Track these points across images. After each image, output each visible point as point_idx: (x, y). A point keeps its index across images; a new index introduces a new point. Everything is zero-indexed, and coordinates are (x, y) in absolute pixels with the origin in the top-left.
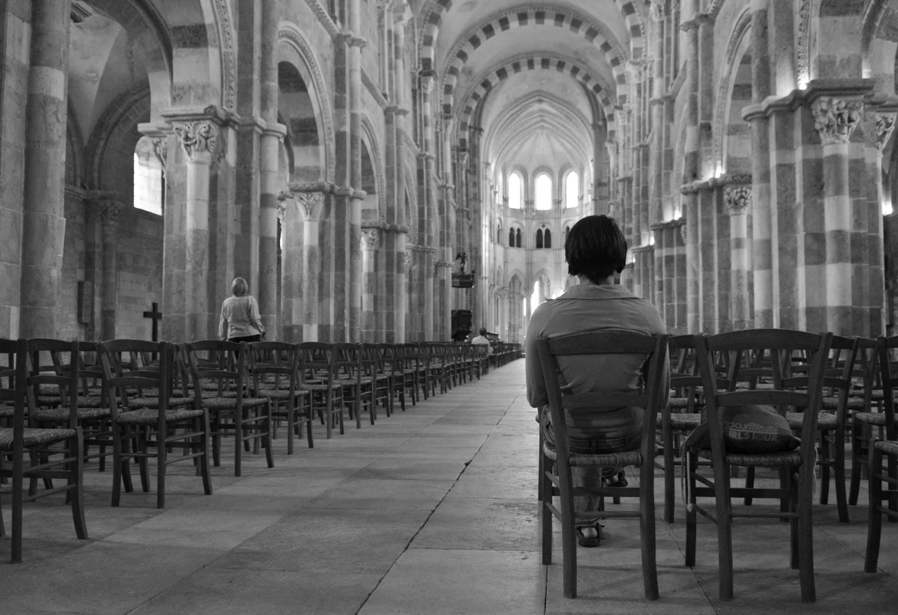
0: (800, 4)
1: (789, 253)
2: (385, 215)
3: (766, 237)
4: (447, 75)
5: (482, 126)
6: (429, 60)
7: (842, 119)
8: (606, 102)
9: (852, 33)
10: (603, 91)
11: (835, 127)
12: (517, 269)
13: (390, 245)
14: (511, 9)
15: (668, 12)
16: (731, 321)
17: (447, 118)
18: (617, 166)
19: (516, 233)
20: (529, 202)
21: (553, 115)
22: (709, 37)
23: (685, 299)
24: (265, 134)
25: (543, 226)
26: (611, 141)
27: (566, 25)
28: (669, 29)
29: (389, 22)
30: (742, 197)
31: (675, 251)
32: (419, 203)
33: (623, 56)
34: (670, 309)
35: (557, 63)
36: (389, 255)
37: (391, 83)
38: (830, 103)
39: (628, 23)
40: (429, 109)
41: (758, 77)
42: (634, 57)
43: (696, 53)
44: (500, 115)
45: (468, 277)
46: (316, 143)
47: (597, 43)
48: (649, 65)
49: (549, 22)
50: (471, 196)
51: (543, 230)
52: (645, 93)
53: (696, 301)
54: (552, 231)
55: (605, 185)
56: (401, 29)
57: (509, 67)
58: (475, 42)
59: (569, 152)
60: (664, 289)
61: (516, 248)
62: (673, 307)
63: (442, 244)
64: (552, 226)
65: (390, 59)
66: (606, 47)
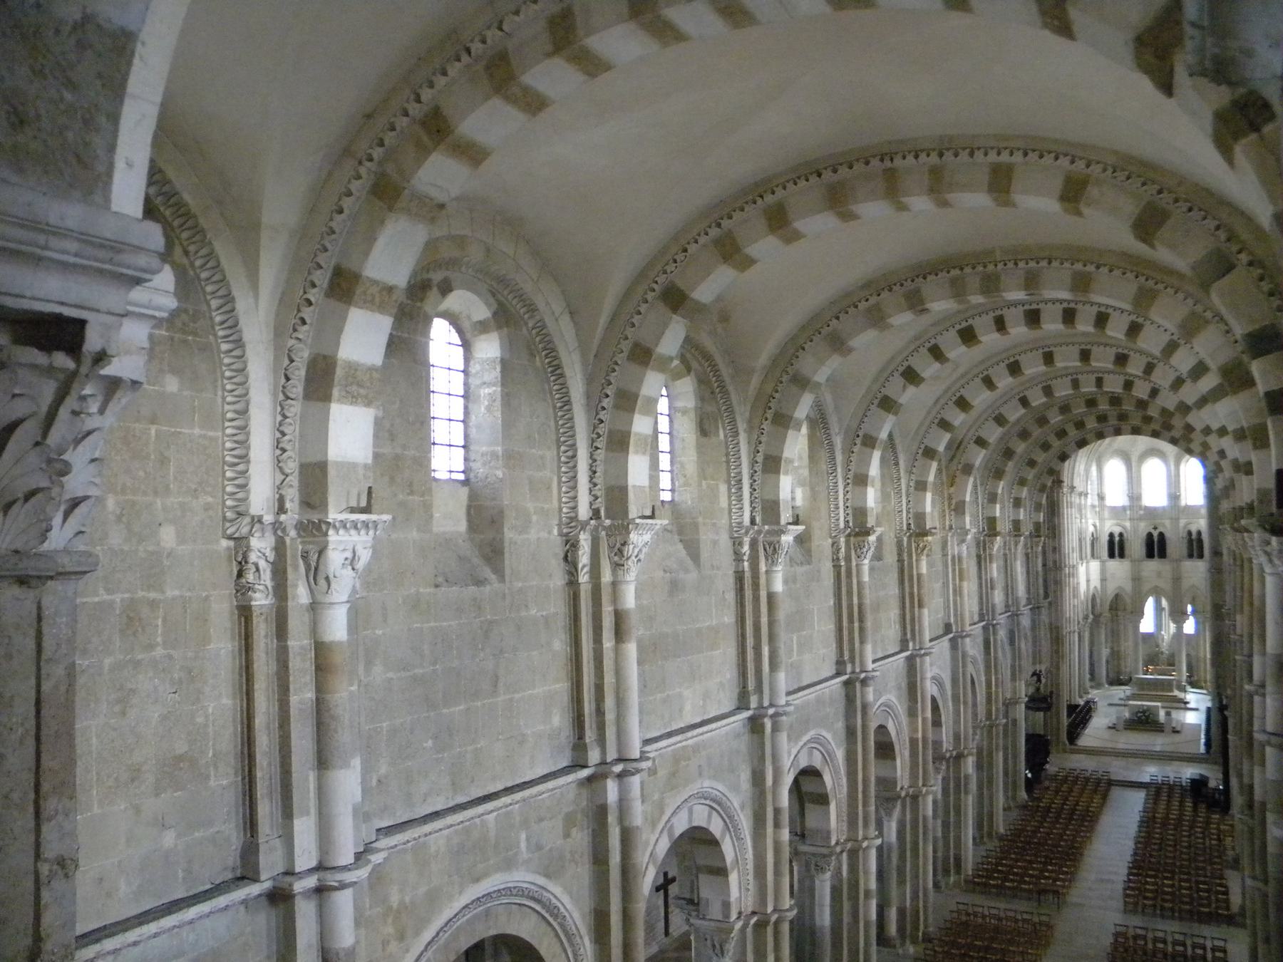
2: (951, 741)
4: (1015, 487)
6: (994, 518)
12: (1120, 588)
19: (1117, 539)
20: (1135, 497)
25: (1155, 528)
29: (953, 548)
32: (986, 675)
37: (956, 610)
46: (894, 759)
50: (1050, 564)
51: (1155, 534)
54: (1167, 535)
56: (965, 548)
61: (1117, 558)
63: (1013, 678)
64: (1167, 528)
65: (954, 585)
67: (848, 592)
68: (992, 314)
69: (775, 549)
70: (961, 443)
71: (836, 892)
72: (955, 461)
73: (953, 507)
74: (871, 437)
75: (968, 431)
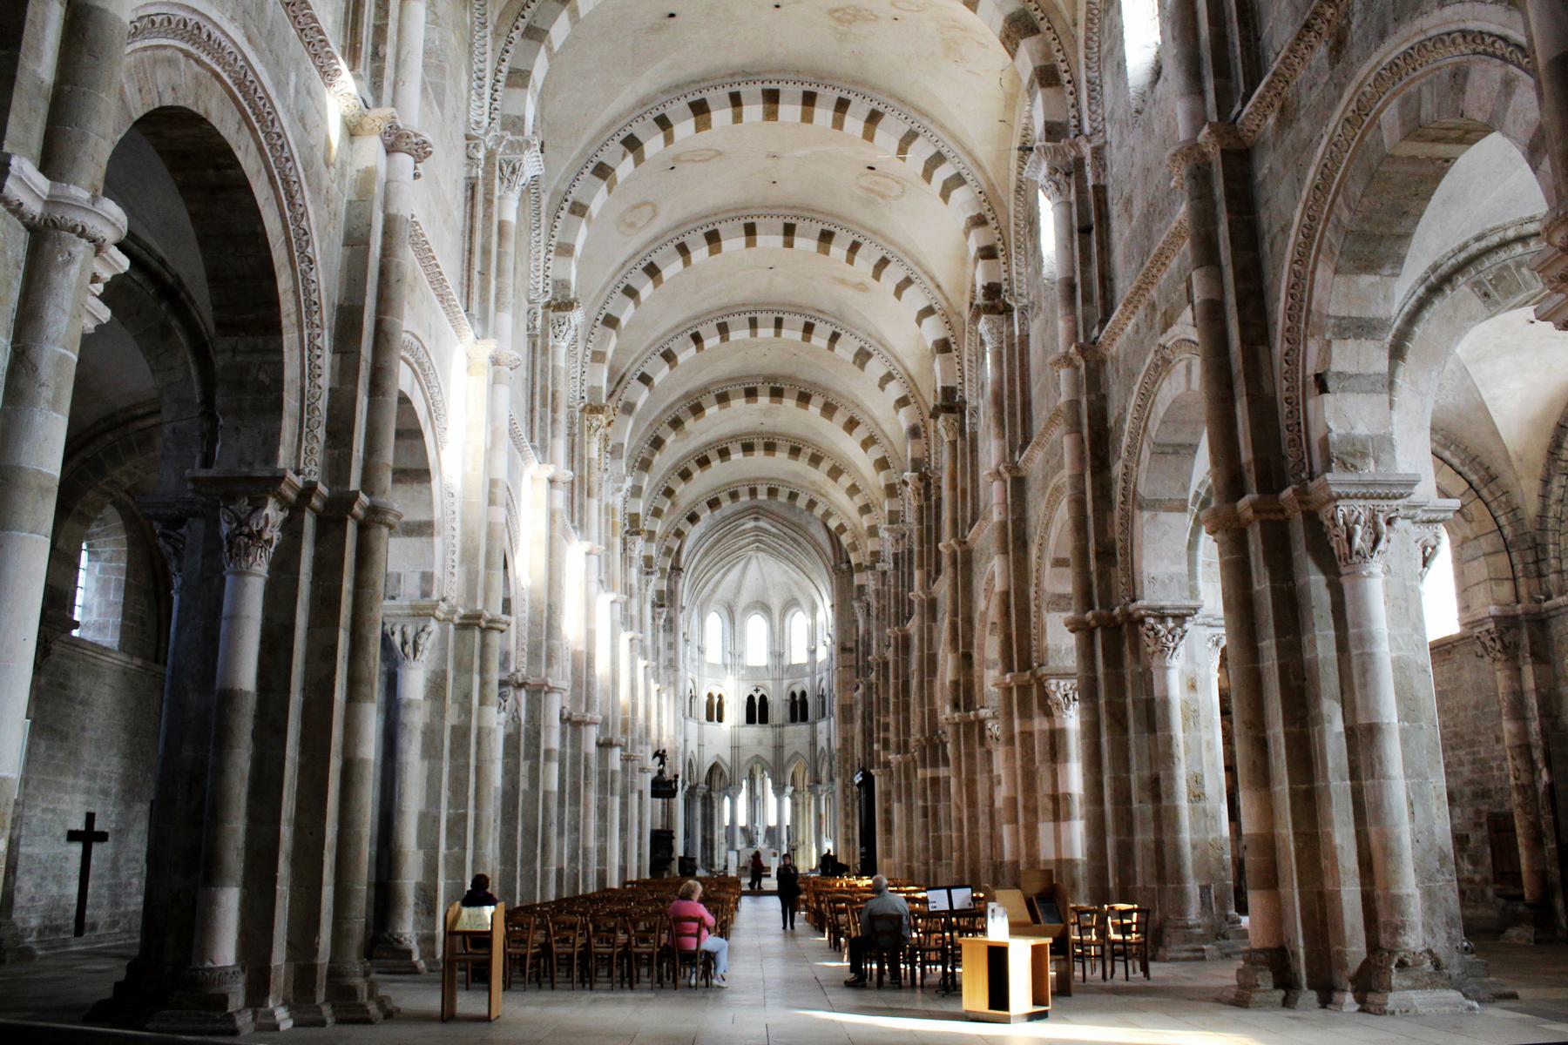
1: (1032, 811)
3: (1012, 794)
4: (649, 518)
12: (718, 756)
13: (603, 760)
14: (734, 438)
15: (927, 497)
17: (647, 573)
18: (868, 632)
21: (774, 535)
24: (551, 690)
25: (757, 690)
26: (859, 598)
28: (929, 515)
31: (942, 772)
36: (603, 773)
37: (607, 566)
38: (1058, 685)
39: (881, 479)
40: (634, 572)
42: (891, 522)
43: (955, 578)
44: (700, 539)
45: (670, 782)
47: (845, 481)
52: (903, 566)
53: (961, 839)
54: (769, 698)
55: (850, 650)
58: (685, 475)
59: (796, 583)
60: (930, 815)
62: (939, 837)
65: (607, 538)
66: (853, 490)
67: (542, 371)
68: (728, 89)
69: (514, 169)
70: (622, 377)
71: (511, 743)
72: (615, 398)
73: (609, 449)
74: (581, 205)
75: (632, 364)
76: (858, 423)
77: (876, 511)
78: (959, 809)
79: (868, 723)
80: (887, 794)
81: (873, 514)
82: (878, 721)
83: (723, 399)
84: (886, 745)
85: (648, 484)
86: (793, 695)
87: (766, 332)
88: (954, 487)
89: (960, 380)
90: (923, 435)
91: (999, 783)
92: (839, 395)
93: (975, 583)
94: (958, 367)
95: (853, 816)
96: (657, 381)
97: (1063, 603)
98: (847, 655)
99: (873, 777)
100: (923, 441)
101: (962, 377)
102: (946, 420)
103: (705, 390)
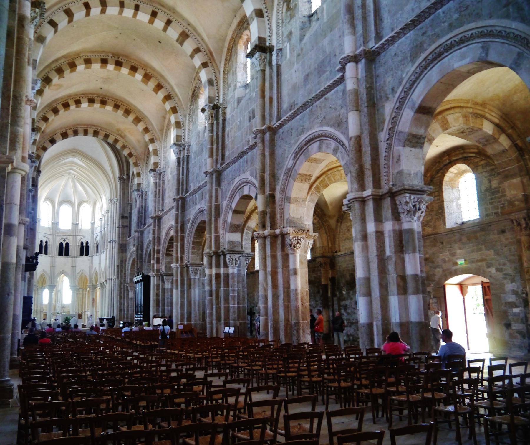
0: (385, 136)
5: (41, 169)
7: (416, 207)
8: (136, 165)
9: (418, 159)
10: (134, 157)
11: (412, 212)
12: (44, 271)
14: (84, 95)
15: (217, 118)
16: (291, 322)
19: (44, 244)
20: (55, 224)
22: (272, 141)
23: (228, 303)
25: (64, 240)
26: (138, 190)
27: (120, 112)
28: (218, 129)
30: (298, 243)
31: (222, 271)
33: (157, 137)
34: (218, 309)
35: (104, 135)
38: (410, 197)
41: (358, 176)
42: (177, 140)
48: (187, 147)
49: (109, 108)
55: (126, 218)
57: (70, 132)
58: (56, 111)
61: (43, 255)
62: (220, 308)
66: (146, 130)
76: (162, 87)
77: (157, 142)
78: (266, 290)
79: (139, 252)
80: (158, 286)
81: (156, 143)
82: (154, 249)
83: (88, 62)
84: (158, 261)
85: (41, 103)
86: (82, 243)
87: (128, 12)
88: (263, 97)
89: (269, 34)
90: (215, 84)
91: (295, 273)
92: (154, 70)
93: (279, 152)
94: (268, 26)
95: (124, 298)
96: (60, 27)
97: (414, 141)
98: (125, 220)
99: (150, 277)
100: (215, 88)
101: (271, 32)
102: (261, 56)
103: (78, 55)
